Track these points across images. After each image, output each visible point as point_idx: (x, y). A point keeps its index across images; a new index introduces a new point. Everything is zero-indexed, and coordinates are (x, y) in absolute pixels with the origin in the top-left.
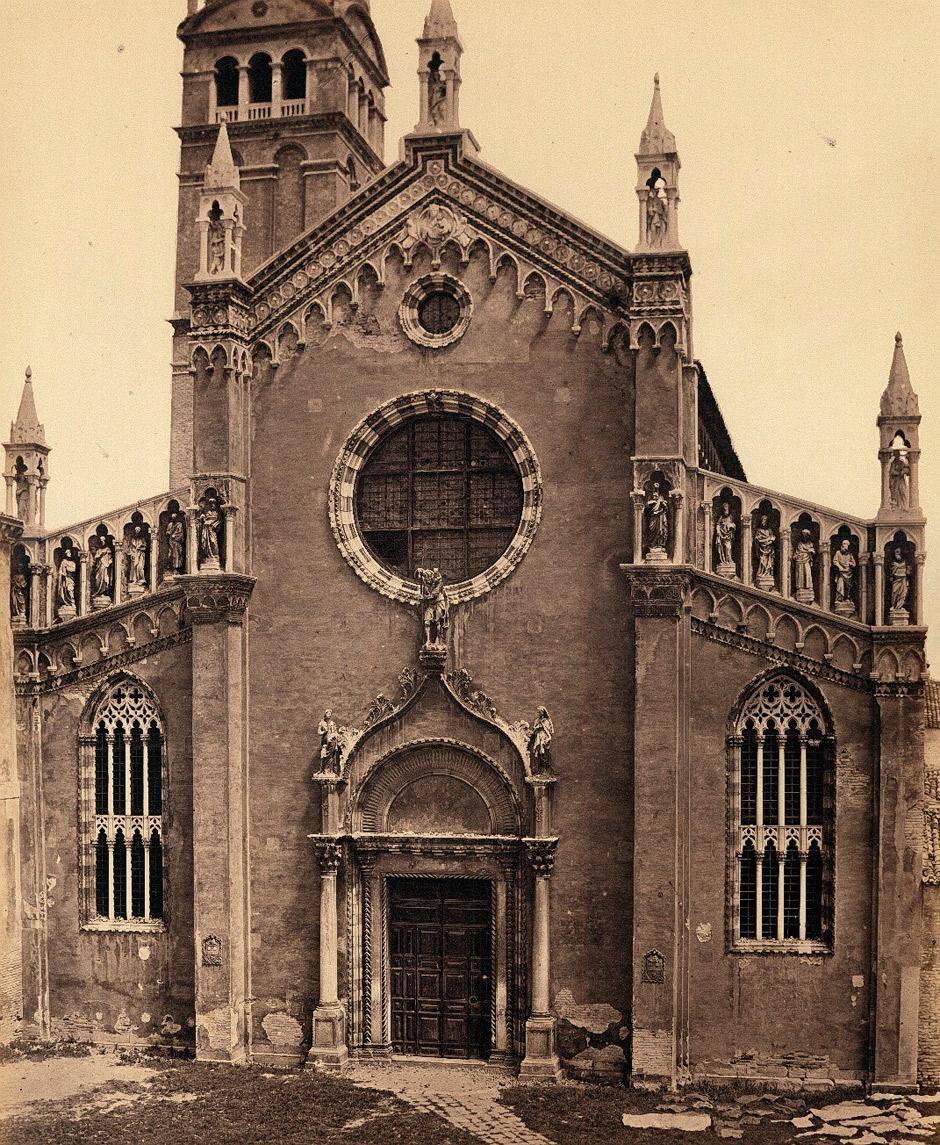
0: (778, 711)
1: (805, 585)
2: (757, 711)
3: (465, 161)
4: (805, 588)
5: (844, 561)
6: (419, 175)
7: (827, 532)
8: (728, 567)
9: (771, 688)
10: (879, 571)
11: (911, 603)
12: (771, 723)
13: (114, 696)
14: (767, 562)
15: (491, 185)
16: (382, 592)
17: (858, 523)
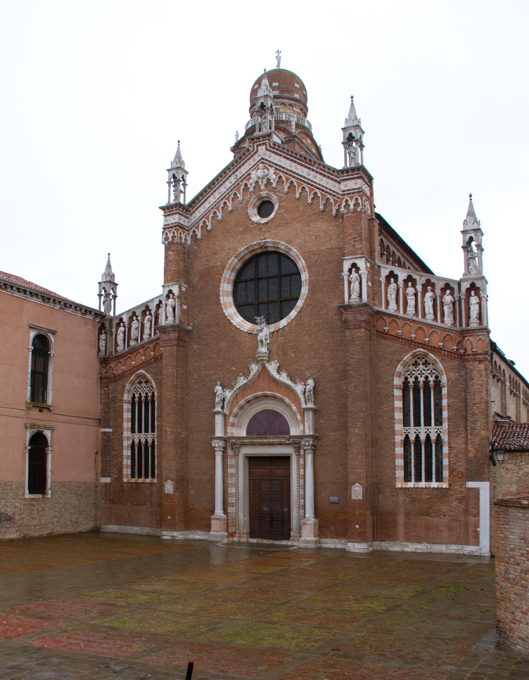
0: (419, 372)
2: (409, 372)
3: (274, 144)
6: (256, 153)
7: (439, 286)
9: (416, 362)
10: (463, 301)
11: (480, 317)
12: (416, 378)
13: (139, 383)
15: (284, 153)
16: (242, 329)
17: (453, 281)
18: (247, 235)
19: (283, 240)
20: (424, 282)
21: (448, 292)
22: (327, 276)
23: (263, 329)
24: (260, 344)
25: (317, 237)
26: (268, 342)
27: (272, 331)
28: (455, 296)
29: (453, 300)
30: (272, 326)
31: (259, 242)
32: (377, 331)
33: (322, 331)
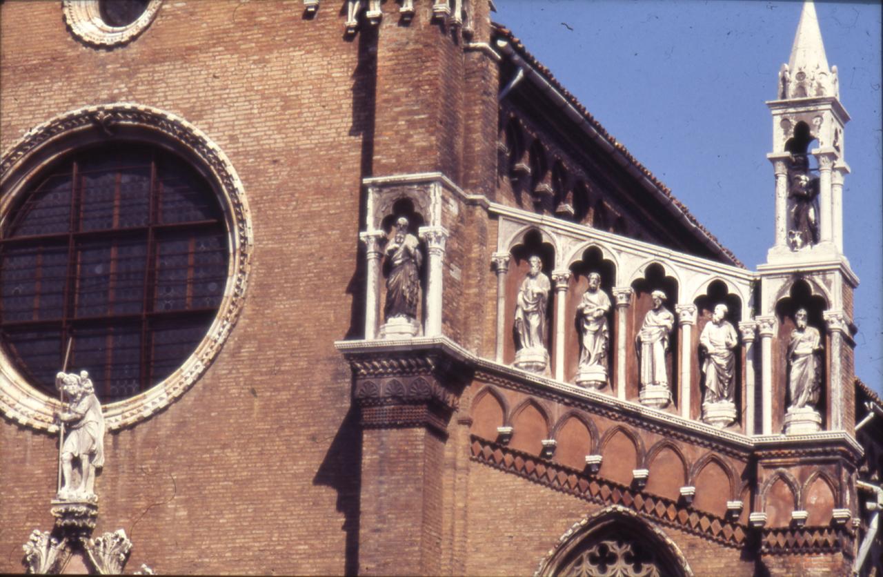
1: (653, 377)
4: (654, 383)
5: (718, 337)
8: (533, 351)
9: (604, 549)
14: (593, 344)
18: (53, 79)
19: (175, 107)
20: (642, 275)
21: (721, 309)
22: (312, 237)
23: (83, 417)
24: (67, 468)
25: (287, 103)
26: (100, 461)
27: (115, 426)
28: (741, 325)
29: (734, 343)
30: (117, 406)
31: (92, 108)
32: (474, 439)
33: (287, 432)
